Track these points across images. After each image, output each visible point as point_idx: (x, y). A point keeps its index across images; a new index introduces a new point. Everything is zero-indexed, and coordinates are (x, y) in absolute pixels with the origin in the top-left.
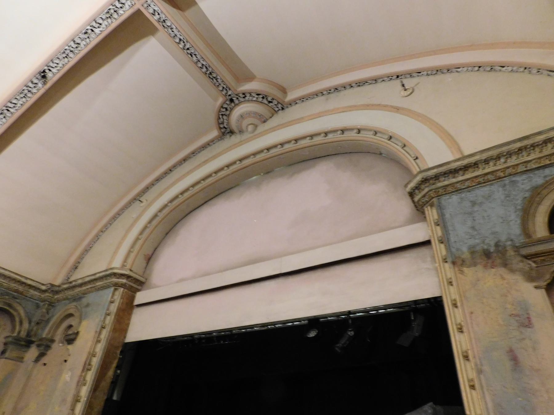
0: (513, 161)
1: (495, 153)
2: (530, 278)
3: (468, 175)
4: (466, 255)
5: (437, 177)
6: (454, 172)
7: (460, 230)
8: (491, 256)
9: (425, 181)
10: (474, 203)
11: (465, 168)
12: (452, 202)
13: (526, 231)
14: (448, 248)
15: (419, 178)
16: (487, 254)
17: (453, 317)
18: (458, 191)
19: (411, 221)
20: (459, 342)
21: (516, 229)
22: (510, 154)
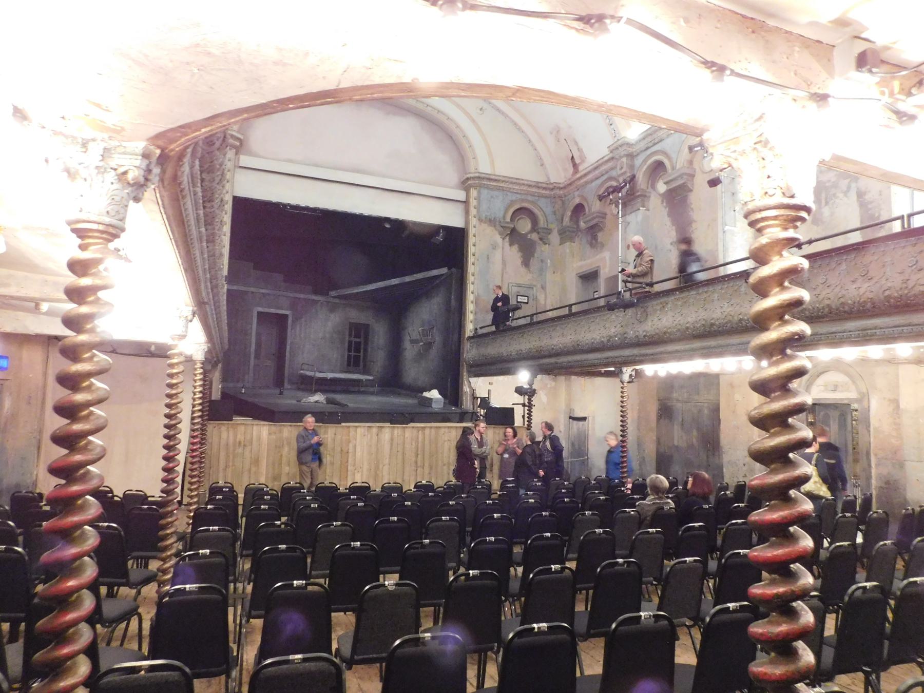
0: (511, 186)
1: (507, 179)
2: (500, 234)
3: (494, 184)
4: (483, 218)
5: (483, 178)
6: (489, 179)
7: (484, 206)
8: (491, 222)
9: (479, 177)
10: (492, 197)
11: (495, 180)
12: (485, 192)
13: (504, 217)
14: (478, 212)
15: (477, 175)
16: (490, 220)
17: (471, 240)
18: (488, 188)
19: (457, 188)
20: (471, 249)
21: (502, 213)
22: (512, 183)
